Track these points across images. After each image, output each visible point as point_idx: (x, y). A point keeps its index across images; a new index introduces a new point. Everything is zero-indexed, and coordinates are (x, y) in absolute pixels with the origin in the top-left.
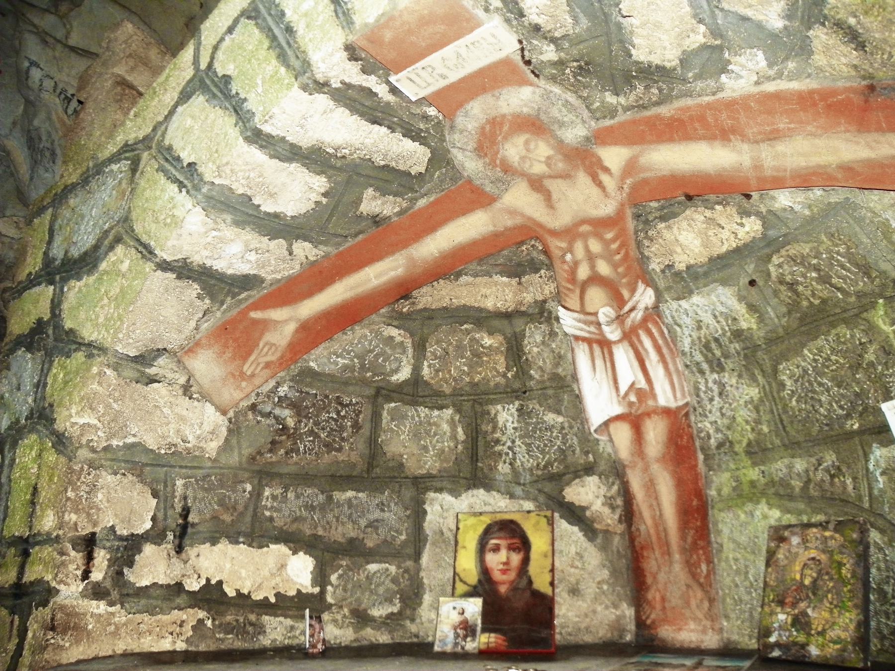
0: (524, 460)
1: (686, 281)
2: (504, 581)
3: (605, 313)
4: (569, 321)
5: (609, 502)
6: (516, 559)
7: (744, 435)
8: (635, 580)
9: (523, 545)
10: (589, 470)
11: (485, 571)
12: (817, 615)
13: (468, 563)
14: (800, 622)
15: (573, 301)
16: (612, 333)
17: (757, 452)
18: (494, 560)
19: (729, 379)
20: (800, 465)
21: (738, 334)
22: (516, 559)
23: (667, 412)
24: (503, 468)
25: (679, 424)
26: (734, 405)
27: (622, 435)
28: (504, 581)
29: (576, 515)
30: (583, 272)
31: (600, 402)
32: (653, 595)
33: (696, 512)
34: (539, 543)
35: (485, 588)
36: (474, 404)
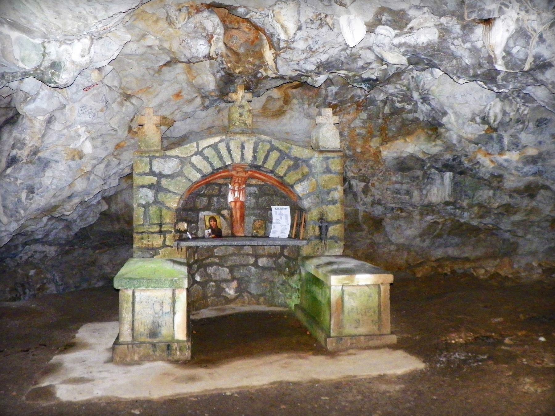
0: (216, 207)
1: (250, 185)
2: (214, 227)
3: (237, 187)
4: (230, 186)
5: (228, 214)
6: (215, 223)
7: (252, 206)
8: (232, 226)
9: (216, 221)
10: (226, 209)
11: (211, 225)
12: (259, 231)
13: (207, 223)
14: (257, 232)
15: (232, 184)
16: (236, 189)
17: (253, 209)
18: (212, 223)
19: (252, 199)
20: (259, 211)
21: (255, 193)
22: (215, 223)
23: (241, 201)
24: (212, 208)
25: (242, 203)
26: (252, 201)
27: (233, 204)
28: (214, 227)
29: (223, 216)
30: (236, 181)
31: (230, 198)
32: (234, 229)
33: (242, 217)
34: (218, 220)
35: (211, 227)
36: (210, 197)
